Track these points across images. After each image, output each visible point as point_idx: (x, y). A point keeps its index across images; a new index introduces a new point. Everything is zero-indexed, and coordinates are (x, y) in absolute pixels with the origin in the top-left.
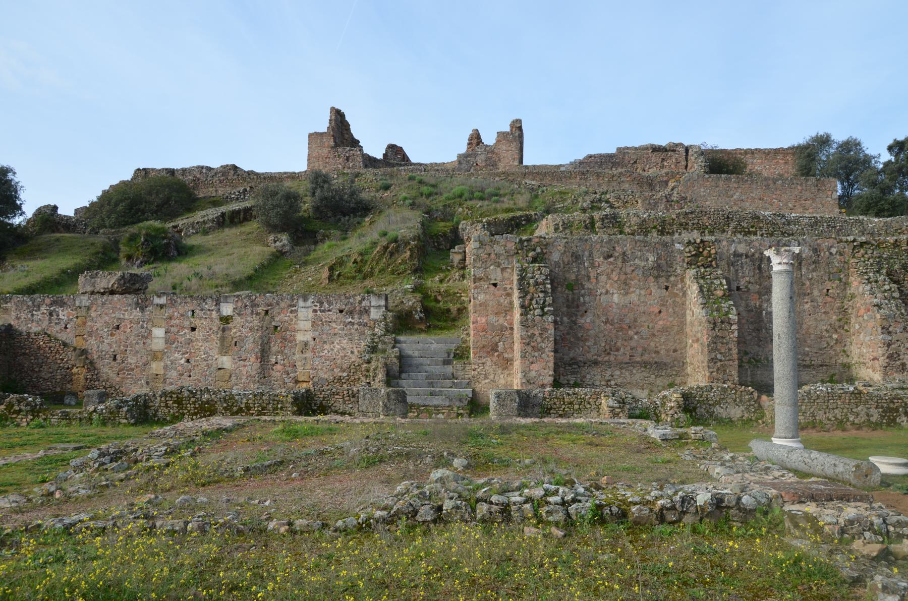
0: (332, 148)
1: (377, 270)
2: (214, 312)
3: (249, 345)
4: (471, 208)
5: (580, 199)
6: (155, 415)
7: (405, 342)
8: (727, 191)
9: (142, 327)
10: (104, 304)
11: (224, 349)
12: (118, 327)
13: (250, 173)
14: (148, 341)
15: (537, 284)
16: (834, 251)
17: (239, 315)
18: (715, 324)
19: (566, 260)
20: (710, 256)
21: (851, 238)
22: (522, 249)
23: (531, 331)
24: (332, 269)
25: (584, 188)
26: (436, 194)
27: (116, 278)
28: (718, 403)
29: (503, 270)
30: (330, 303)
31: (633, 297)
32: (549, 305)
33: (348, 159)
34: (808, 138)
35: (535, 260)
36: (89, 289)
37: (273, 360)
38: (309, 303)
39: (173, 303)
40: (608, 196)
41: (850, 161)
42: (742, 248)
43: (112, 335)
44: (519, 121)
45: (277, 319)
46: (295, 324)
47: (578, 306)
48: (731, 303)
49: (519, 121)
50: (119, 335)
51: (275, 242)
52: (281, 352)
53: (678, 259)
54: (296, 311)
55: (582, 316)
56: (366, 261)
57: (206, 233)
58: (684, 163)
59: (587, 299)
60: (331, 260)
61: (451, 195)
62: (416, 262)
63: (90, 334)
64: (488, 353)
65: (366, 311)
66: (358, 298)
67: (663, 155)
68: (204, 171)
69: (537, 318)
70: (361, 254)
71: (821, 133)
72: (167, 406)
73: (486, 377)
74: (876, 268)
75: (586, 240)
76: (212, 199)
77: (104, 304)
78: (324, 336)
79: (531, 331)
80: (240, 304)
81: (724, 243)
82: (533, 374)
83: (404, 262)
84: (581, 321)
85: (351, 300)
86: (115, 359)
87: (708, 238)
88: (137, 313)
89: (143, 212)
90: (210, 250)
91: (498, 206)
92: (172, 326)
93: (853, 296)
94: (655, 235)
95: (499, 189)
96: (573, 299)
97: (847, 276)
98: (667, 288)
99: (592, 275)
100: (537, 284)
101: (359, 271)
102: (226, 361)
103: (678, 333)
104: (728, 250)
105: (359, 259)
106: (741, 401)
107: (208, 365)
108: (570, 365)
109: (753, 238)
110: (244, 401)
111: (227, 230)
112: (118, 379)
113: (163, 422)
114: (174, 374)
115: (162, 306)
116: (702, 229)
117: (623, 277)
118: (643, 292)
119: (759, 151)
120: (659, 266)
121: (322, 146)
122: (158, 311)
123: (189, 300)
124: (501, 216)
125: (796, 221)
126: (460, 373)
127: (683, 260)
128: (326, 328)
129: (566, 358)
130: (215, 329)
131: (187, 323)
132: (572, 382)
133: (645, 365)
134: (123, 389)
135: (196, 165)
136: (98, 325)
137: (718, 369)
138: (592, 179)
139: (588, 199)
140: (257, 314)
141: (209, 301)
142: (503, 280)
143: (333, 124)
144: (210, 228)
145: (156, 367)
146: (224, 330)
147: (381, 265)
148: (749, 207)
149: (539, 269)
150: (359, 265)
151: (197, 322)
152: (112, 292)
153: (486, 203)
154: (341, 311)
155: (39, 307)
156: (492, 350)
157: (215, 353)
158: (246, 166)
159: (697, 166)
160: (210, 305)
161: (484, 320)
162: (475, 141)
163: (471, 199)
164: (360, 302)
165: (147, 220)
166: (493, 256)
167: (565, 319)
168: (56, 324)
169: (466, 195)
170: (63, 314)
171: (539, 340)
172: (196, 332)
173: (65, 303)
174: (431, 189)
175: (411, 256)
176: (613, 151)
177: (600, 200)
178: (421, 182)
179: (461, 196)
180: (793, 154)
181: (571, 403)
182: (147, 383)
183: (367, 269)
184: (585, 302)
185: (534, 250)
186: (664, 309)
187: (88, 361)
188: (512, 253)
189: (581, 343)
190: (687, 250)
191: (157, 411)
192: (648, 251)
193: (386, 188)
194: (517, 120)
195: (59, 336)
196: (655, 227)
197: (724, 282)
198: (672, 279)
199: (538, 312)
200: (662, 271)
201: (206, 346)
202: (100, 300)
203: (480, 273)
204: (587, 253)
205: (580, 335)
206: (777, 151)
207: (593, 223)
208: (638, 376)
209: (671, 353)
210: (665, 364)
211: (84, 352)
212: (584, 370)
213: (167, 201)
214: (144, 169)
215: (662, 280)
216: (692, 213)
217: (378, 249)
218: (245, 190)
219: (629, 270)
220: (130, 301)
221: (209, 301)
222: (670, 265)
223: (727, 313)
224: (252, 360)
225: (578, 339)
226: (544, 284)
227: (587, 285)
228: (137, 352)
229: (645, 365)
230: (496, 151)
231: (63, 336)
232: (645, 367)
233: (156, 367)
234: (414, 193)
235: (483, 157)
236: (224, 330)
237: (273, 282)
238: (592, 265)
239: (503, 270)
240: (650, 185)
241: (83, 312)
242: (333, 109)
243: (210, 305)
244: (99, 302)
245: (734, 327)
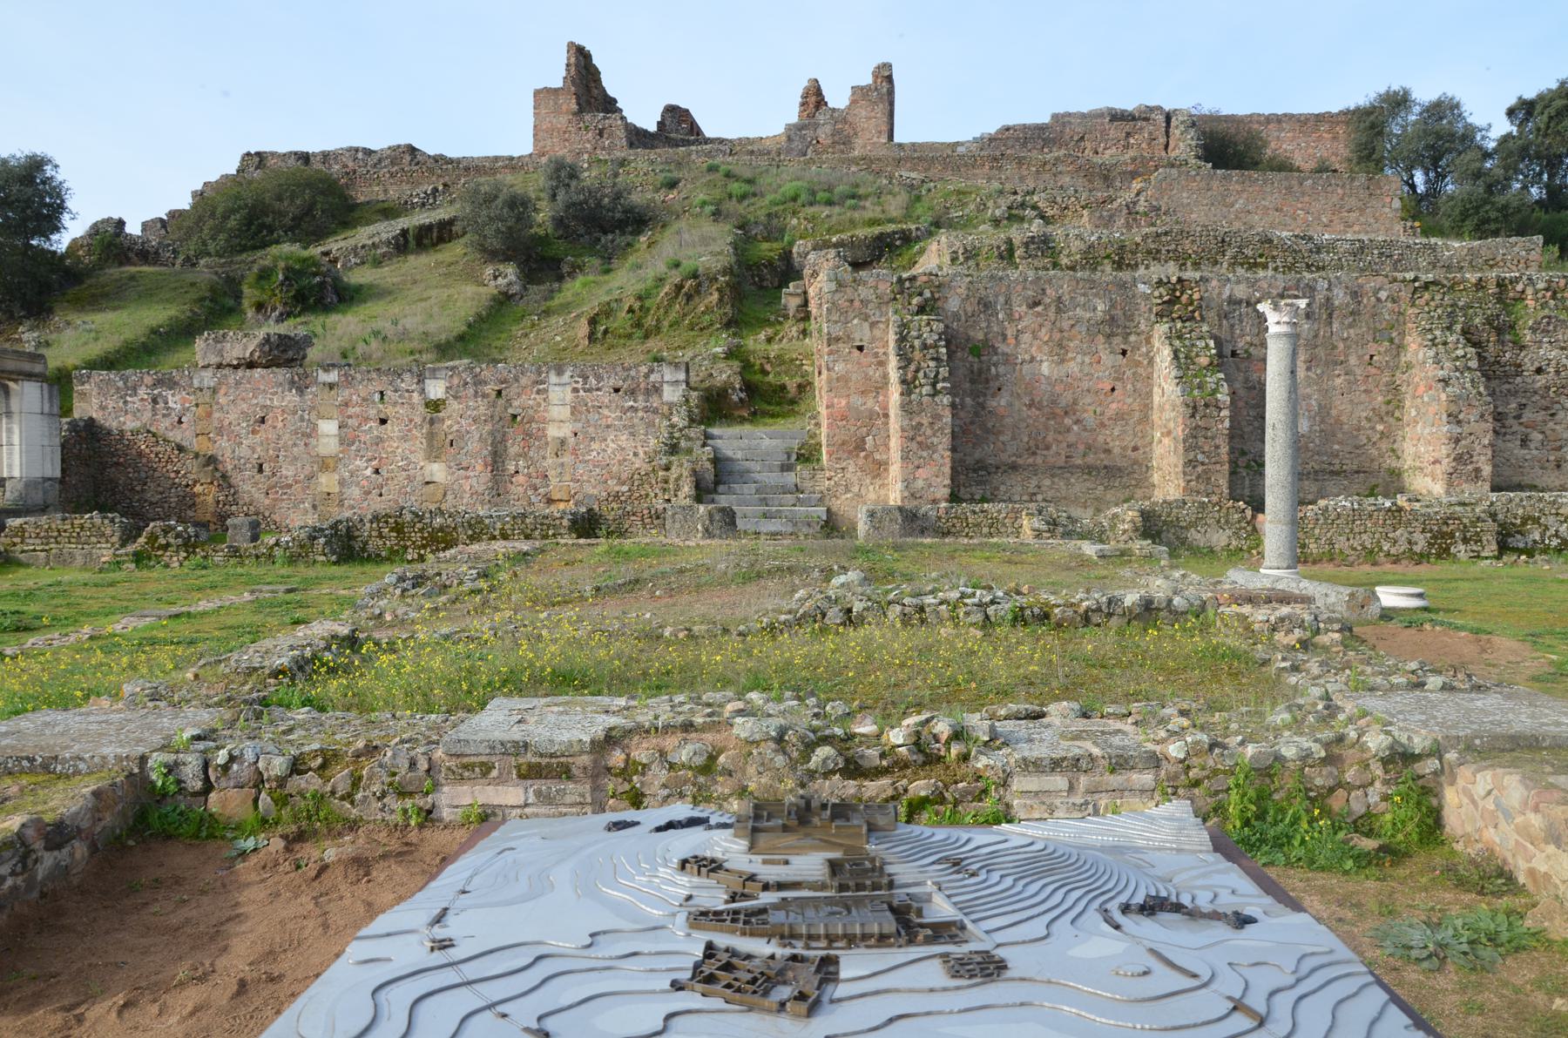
0: (575, 114)
1: (666, 323)
2: (415, 395)
3: (473, 445)
4: (811, 219)
5: (990, 204)
6: (364, 549)
7: (720, 438)
8: (1224, 197)
9: (302, 419)
10: (238, 383)
11: (433, 454)
12: (263, 420)
13: (439, 159)
14: (313, 441)
15: (925, 346)
16: (1383, 295)
17: (455, 397)
18: (1195, 407)
19: (969, 309)
20: (1191, 304)
21: (1410, 275)
22: (901, 293)
23: (917, 419)
24: (593, 322)
25: (996, 185)
26: (755, 195)
27: (256, 342)
28: (1193, 524)
29: (873, 325)
30: (599, 378)
31: (1073, 367)
32: (944, 380)
33: (601, 134)
34: (1373, 96)
35: (921, 310)
36: (214, 360)
37: (512, 469)
38: (566, 377)
39: (349, 381)
40: (1036, 198)
41: (1442, 135)
43: (254, 432)
44: (888, 66)
45: (516, 403)
46: (546, 411)
47: (987, 381)
48: (1222, 376)
49: (888, 66)
50: (265, 432)
51: (496, 278)
52: (525, 455)
53: (1143, 308)
54: (546, 391)
55: (994, 395)
56: (648, 310)
57: (378, 263)
58: (1162, 140)
59: (1001, 369)
60: (590, 307)
61: (778, 197)
62: (728, 309)
63: (220, 431)
64: (850, 452)
65: (657, 390)
66: (644, 369)
67: (1128, 127)
68: (360, 155)
69: (926, 399)
70: (640, 298)
71: (1395, 87)
72: (381, 536)
73: (847, 490)
74: (1446, 322)
75: (1001, 279)
76: (380, 206)
77: (238, 383)
78: (591, 430)
79: (917, 419)
80: (456, 381)
81: (1214, 283)
82: (920, 483)
83: (708, 310)
84: (992, 403)
85: (633, 373)
86: (260, 470)
87: (1190, 274)
88: (292, 397)
89: (271, 230)
90: (390, 293)
91: (856, 215)
92: (350, 417)
93: (1409, 366)
94: (1108, 269)
95: (857, 186)
96: (980, 371)
97: (1402, 334)
98: (1124, 353)
99: (1009, 333)
100: (925, 346)
101: (638, 325)
102: (438, 471)
103: (1140, 421)
104: (1220, 294)
105: (637, 305)
106: (1227, 522)
107: (408, 477)
108: (975, 471)
109: (1261, 273)
110: (499, 525)
111: (411, 258)
112: (267, 502)
113: (377, 559)
114: (356, 492)
115: (331, 386)
116: (1181, 260)
117: (1057, 336)
118: (1087, 360)
119: (1290, 117)
120: (1112, 318)
121: (557, 111)
122: (326, 394)
123: (374, 375)
124: (862, 232)
125: (1331, 247)
126: (808, 484)
127: (1150, 310)
128: (593, 417)
129: (969, 461)
130: (418, 420)
131: (372, 412)
132: (977, 497)
133: (1089, 470)
134: (276, 517)
135: (345, 145)
136: (232, 417)
137: (1198, 477)
138: (1010, 169)
139: (1004, 203)
140: (484, 396)
141: (407, 376)
142: (873, 340)
143: (573, 72)
144: (384, 255)
145: (328, 482)
146: (432, 422)
147: (673, 316)
148: (1260, 224)
149: (928, 324)
150: (638, 316)
151: (389, 411)
152: (251, 365)
153: (837, 209)
154: (617, 390)
155: (135, 390)
156: (856, 448)
157: (419, 458)
158: (430, 148)
159: (1184, 145)
160: (408, 382)
161: (844, 402)
162: (813, 99)
163: (811, 204)
164: (647, 376)
165: (277, 242)
166: (857, 303)
167: (968, 400)
168: (164, 416)
169: (804, 197)
170: (174, 400)
171: (929, 432)
172: (388, 425)
173: (176, 383)
174: (746, 188)
175: (721, 300)
176: (1045, 119)
177: (1023, 205)
178: (728, 175)
179: (794, 199)
180: (1347, 123)
181: (978, 525)
182: (314, 507)
184: (998, 375)
185: (921, 294)
186: (1119, 385)
187: (218, 475)
188: (886, 299)
189: (992, 438)
190: (1156, 294)
191: (366, 543)
192: (1096, 295)
193: (672, 185)
194: (884, 65)
195: (170, 435)
196: (1108, 257)
197: (1212, 343)
198: (1132, 338)
199: (926, 390)
200: (1117, 327)
201: (404, 448)
202: (233, 377)
203: (838, 331)
204: (1001, 299)
205: (990, 425)
206: (1320, 118)
207: (1011, 250)
208: (1077, 488)
209: (1129, 452)
210: (1119, 469)
211: (211, 460)
212: (996, 479)
213: (308, 211)
214: (258, 154)
215: (1117, 340)
216: (1166, 234)
217: (666, 289)
218: (435, 190)
219: (1066, 325)
220: (281, 378)
221: (407, 376)
222: (1130, 318)
223: (1215, 391)
224: (479, 468)
225: (988, 431)
226: (936, 346)
227: (1002, 348)
228: (296, 459)
229: (1089, 470)
230: (850, 118)
231: (176, 436)
232: (1089, 473)
233: (328, 482)
234: (717, 193)
235: (828, 129)
236: (432, 422)
237: (499, 343)
238: (1010, 316)
239: (873, 325)
240: (1106, 178)
242: (571, 45)
243: (408, 382)
244: (231, 380)
245: (1225, 413)
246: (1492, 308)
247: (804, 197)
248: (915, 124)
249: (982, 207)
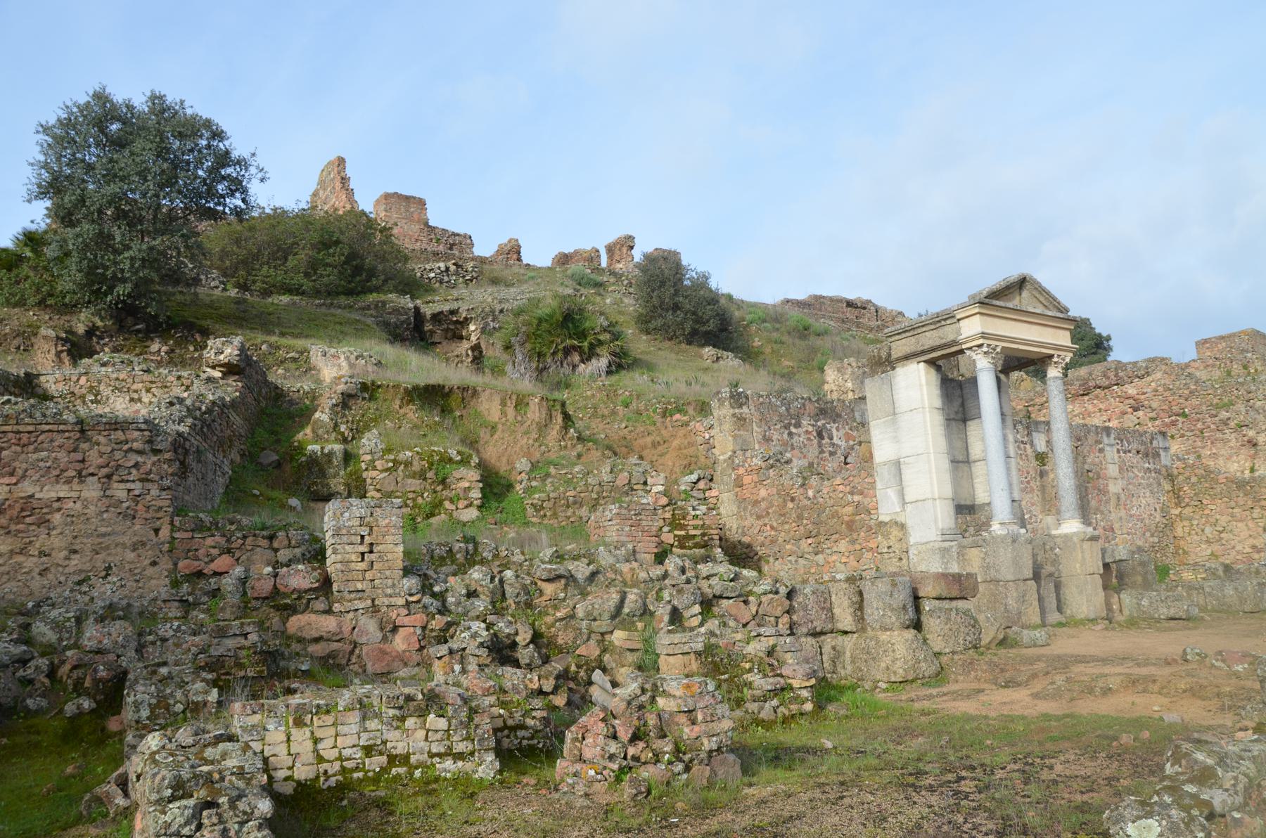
2: (1028, 446)
45: (1089, 460)
121: (410, 219)
165: (377, 289)
168: (831, 454)
218: (447, 269)
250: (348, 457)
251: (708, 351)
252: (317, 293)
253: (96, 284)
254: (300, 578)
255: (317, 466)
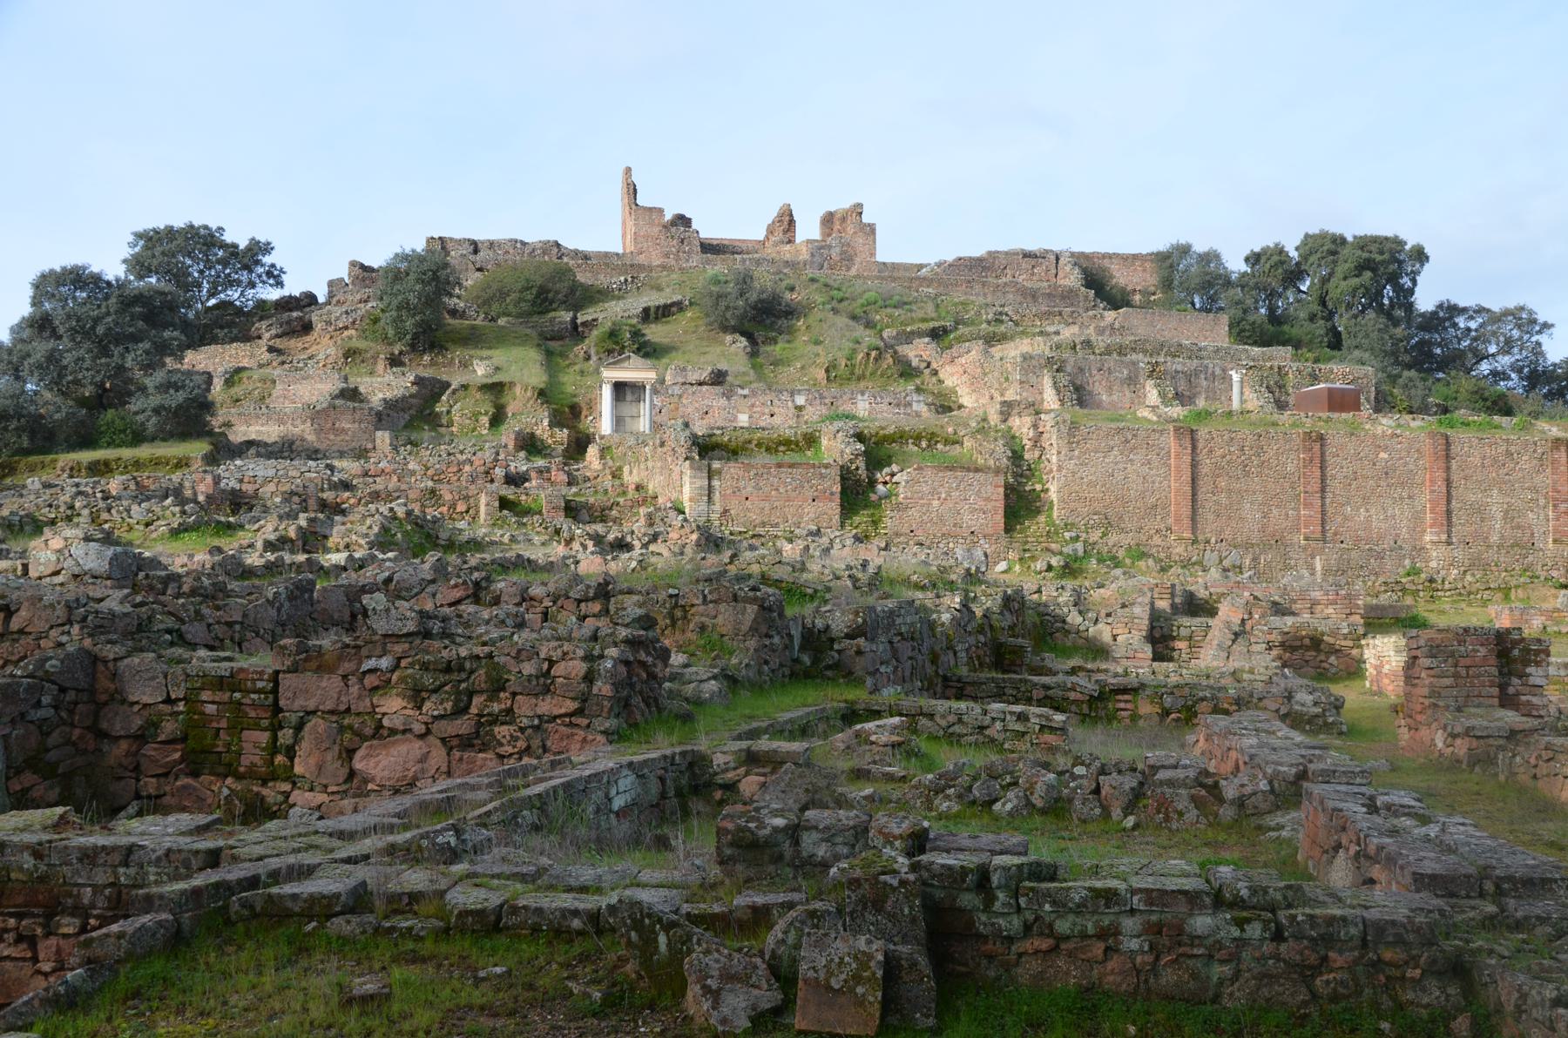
4: (890, 316)
13: (576, 252)
24: (827, 371)
31: (1115, 397)
36: (681, 380)
42: (1179, 368)
44: (860, 205)
49: (860, 205)
65: (910, 405)
67: (1033, 262)
71: (1182, 241)
88: (723, 401)
121: (652, 224)
125: (1205, 349)
138: (977, 287)
151: (776, 410)
152: (700, 384)
159: (1071, 278)
160: (785, 396)
178: (826, 285)
183: (858, 371)
193: (792, 289)
202: (692, 389)
206: (1135, 257)
235: (838, 250)
241: (676, 399)
243: (785, 396)
246: (1277, 378)
247: (880, 303)
248: (889, 250)
249: (978, 314)
250: (449, 412)
251: (729, 338)
252: (519, 316)
253: (400, 336)
254: (370, 446)
255: (438, 415)
